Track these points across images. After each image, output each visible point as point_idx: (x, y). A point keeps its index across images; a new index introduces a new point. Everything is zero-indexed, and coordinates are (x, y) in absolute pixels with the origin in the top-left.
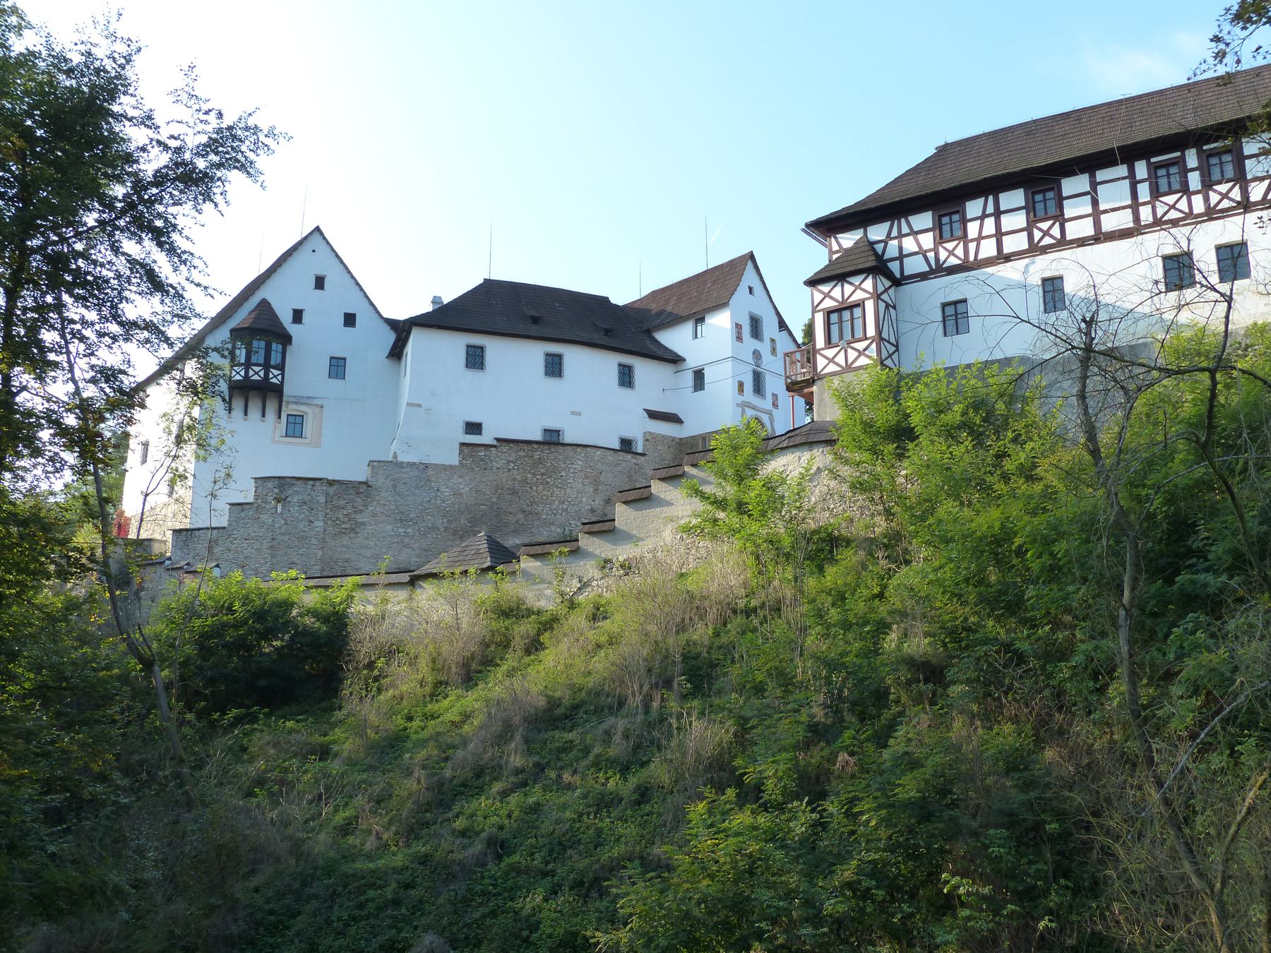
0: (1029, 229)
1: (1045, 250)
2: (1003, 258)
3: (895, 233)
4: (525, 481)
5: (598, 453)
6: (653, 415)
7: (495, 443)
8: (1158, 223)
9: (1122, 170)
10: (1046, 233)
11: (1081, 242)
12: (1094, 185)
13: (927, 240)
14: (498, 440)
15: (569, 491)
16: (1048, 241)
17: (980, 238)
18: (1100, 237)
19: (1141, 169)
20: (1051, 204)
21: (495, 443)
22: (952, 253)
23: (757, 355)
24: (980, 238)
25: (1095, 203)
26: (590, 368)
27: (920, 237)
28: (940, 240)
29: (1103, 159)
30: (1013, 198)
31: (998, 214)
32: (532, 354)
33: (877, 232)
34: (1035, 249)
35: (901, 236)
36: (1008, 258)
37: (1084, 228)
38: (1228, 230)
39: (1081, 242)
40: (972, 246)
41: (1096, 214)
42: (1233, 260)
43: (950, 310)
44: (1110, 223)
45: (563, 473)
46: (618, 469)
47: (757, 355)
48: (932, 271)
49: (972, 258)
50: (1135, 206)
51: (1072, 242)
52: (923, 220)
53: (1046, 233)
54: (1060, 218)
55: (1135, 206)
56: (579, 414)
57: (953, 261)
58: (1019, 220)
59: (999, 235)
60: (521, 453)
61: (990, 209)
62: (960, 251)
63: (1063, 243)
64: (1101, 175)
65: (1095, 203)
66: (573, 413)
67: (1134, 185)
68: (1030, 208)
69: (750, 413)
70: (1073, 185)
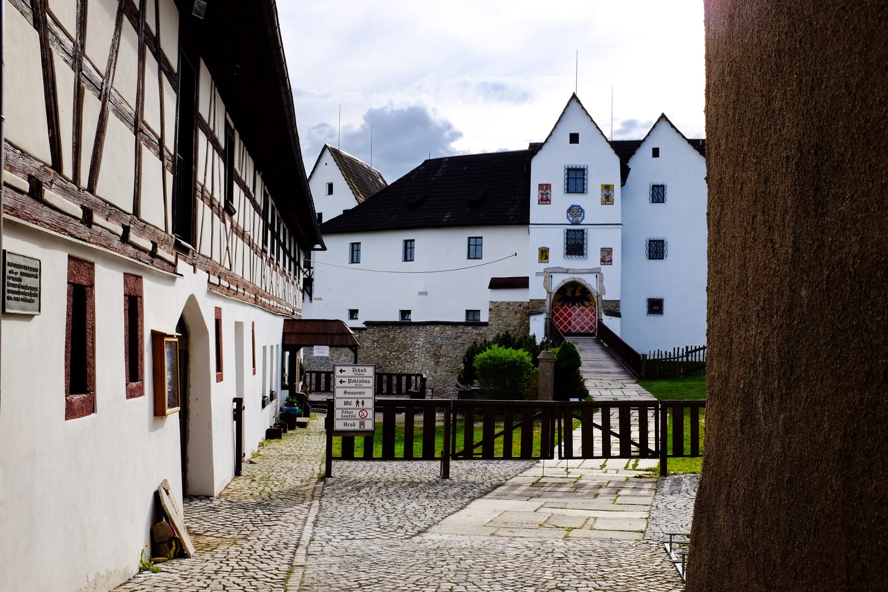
4: (385, 356)
5: (437, 329)
6: (497, 284)
7: (364, 326)
14: (366, 323)
15: (416, 364)
21: (364, 326)
23: (575, 212)
26: (442, 247)
32: (393, 242)
43: (473, 242)
45: (411, 350)
46: (460, 341)
47: (575, 212)
56: (426, 293)
60: (382, 334)
66: (420, 294)
69: (558, 281)
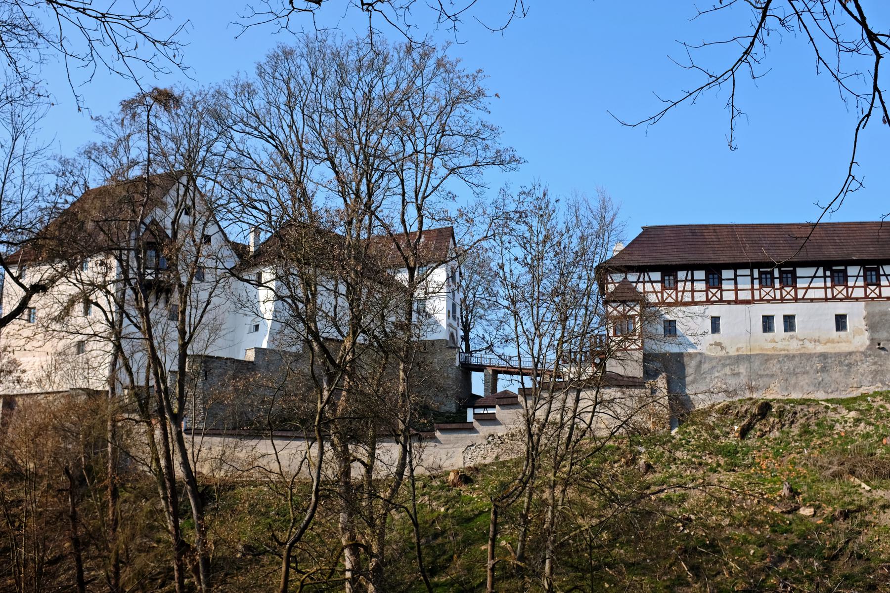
0: (707, 291)
1: (713, 303)
2: (693, 303)
3: (641, 280)
8: (761, 300)
9: (748, 272)
10: (714, 295)
11: (729, 302)
12: (736, 276)
13: (658, 287)
16: (714, 299)
17: (684, 291)
18: (737, 302)
19: (756, 274)
20: (716, 280)
22: (670, 296)
24: (684, 291)
25: (736, 284)
27: (655, 284)
28: (664, 288)
29: (744, 266)
30: (700, 274)
31: (693, 281)
33: (632, 277)
34: (708, 302)
35: (644, 282)
36: (696, 304)
37: (729, 296)
38: (789, 309)
39: (729, 302)
40: (680, 294)
41: (736, 290)
42: (789, 321)
44: (742, 296)
48: (659, 303)
49: (679, 299)
50: (752, 289)
51: (725, 301)
52: (656, 276)
53: (714, 295)
54: (720, 288)
55: (752, 289)
57: (669, 300)
58: (701, 286)
59: (693, 291)
61: (689, 278)
62: (674, 296)
63: (721, 301)
64: (739, 272)
65: (736, 284)
67: (753, 279)
68: (707, 280)
70: (727, 274)
